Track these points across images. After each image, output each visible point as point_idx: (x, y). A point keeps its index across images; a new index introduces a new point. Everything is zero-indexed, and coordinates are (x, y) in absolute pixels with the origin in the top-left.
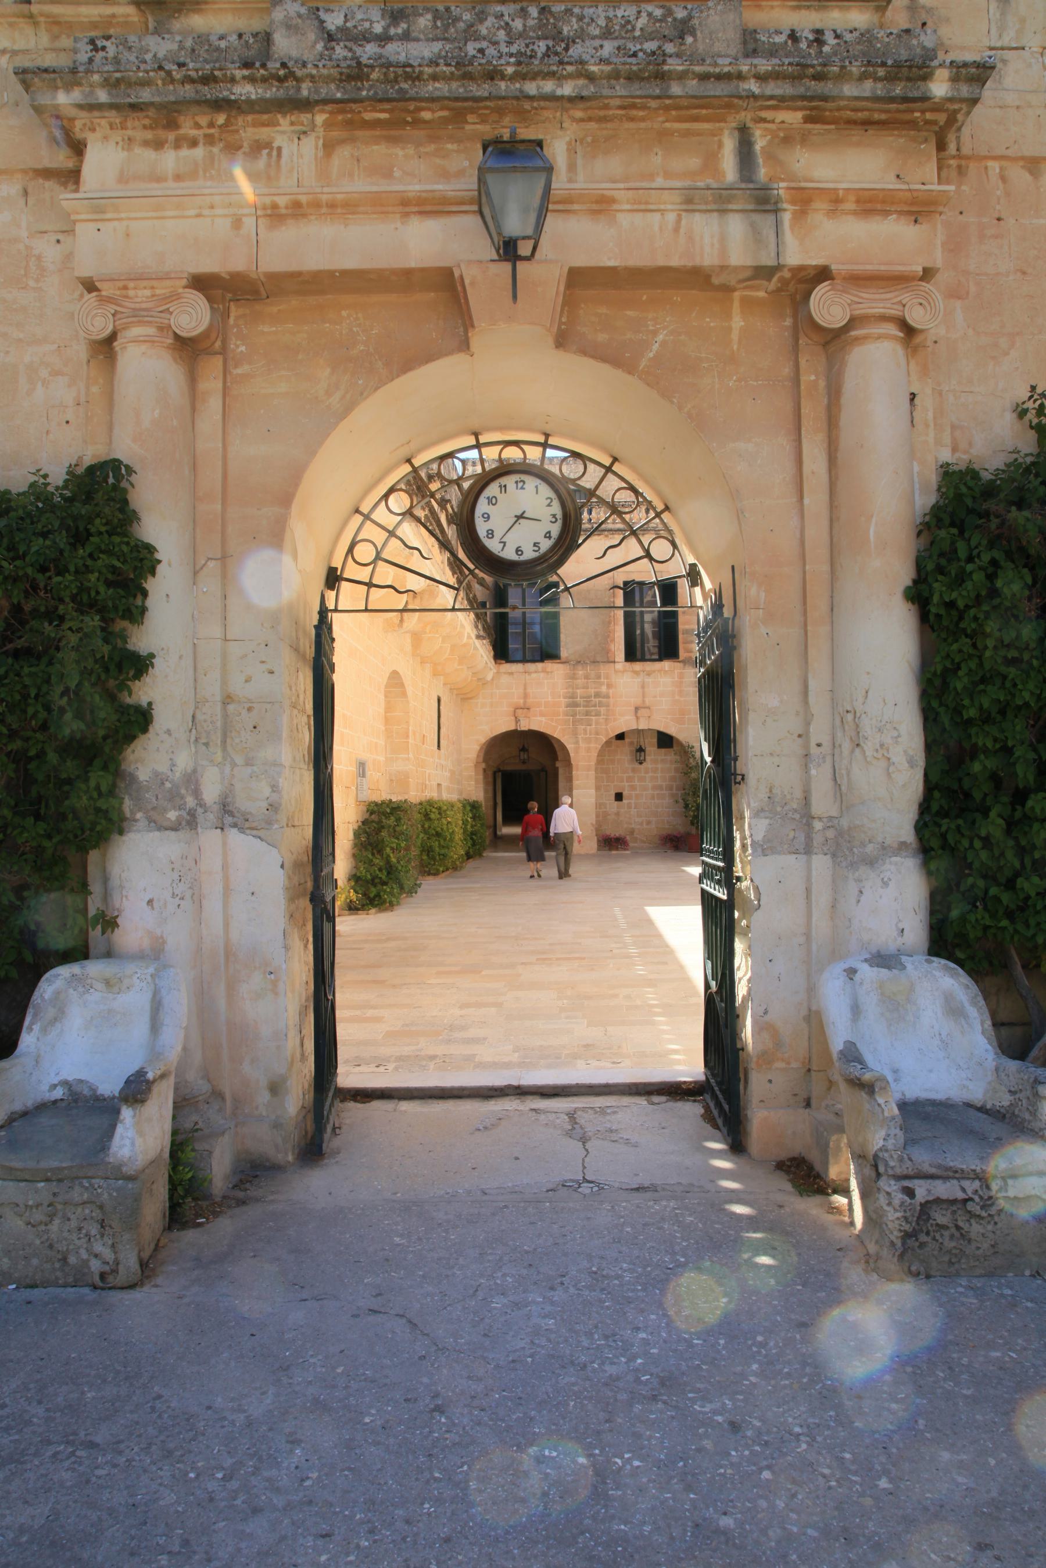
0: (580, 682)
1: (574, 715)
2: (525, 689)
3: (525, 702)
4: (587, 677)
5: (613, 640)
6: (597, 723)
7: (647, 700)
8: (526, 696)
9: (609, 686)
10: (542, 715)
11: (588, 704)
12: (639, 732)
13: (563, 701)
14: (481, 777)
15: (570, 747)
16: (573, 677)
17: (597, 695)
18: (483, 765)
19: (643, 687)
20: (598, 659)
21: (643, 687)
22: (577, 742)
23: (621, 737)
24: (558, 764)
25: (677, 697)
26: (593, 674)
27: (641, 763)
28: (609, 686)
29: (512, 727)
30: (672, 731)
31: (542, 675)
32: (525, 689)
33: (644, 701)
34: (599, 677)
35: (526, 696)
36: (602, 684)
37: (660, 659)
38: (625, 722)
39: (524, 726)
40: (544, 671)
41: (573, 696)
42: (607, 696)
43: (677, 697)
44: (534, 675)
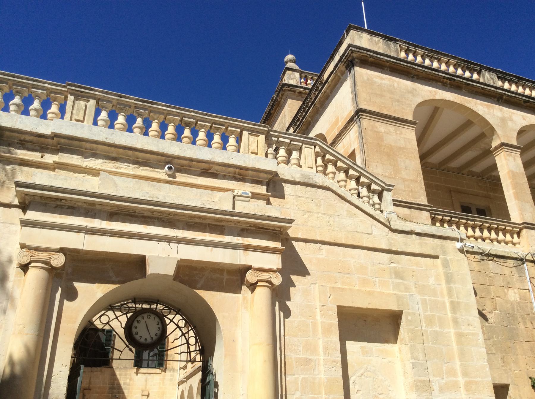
3: (89, 386)
7: (147, 387)
8: (90, 383)
10: (97, 393)
13: (108, 386)
19: (146, 381)
21: (146, 381)
25: (161, 386)
28: (131, 380)
31: (99, 373)
33: (146, 387)
34: (126, 375)
35: (90, 383)
36: (127, 378)
37: (155, 368)
40: (101, 371)
42: (129, 385)
44: (95, 373)
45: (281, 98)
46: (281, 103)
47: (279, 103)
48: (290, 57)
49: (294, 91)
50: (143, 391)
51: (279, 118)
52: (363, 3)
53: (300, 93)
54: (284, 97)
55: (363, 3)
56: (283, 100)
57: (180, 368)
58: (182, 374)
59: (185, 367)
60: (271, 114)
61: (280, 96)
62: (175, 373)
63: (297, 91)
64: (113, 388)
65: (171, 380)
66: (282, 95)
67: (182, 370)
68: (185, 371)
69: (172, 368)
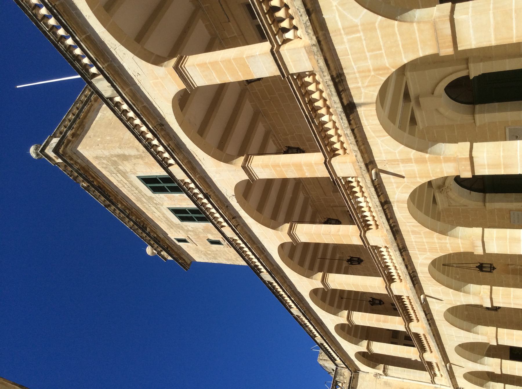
45: (76, 163)
46: (84, 165)
47: (83, 168)
48: (32, 150)
49: (69, 141)
51: (99, 167)
52: (18, 87)
53: (73, 135)
54: (74, 157)
55: (18, 87)
56: (79, 161)
60: (99, 187)
61: (72, 162)
63: (70, 138)
66: (71, 159)
67: (436, 379)
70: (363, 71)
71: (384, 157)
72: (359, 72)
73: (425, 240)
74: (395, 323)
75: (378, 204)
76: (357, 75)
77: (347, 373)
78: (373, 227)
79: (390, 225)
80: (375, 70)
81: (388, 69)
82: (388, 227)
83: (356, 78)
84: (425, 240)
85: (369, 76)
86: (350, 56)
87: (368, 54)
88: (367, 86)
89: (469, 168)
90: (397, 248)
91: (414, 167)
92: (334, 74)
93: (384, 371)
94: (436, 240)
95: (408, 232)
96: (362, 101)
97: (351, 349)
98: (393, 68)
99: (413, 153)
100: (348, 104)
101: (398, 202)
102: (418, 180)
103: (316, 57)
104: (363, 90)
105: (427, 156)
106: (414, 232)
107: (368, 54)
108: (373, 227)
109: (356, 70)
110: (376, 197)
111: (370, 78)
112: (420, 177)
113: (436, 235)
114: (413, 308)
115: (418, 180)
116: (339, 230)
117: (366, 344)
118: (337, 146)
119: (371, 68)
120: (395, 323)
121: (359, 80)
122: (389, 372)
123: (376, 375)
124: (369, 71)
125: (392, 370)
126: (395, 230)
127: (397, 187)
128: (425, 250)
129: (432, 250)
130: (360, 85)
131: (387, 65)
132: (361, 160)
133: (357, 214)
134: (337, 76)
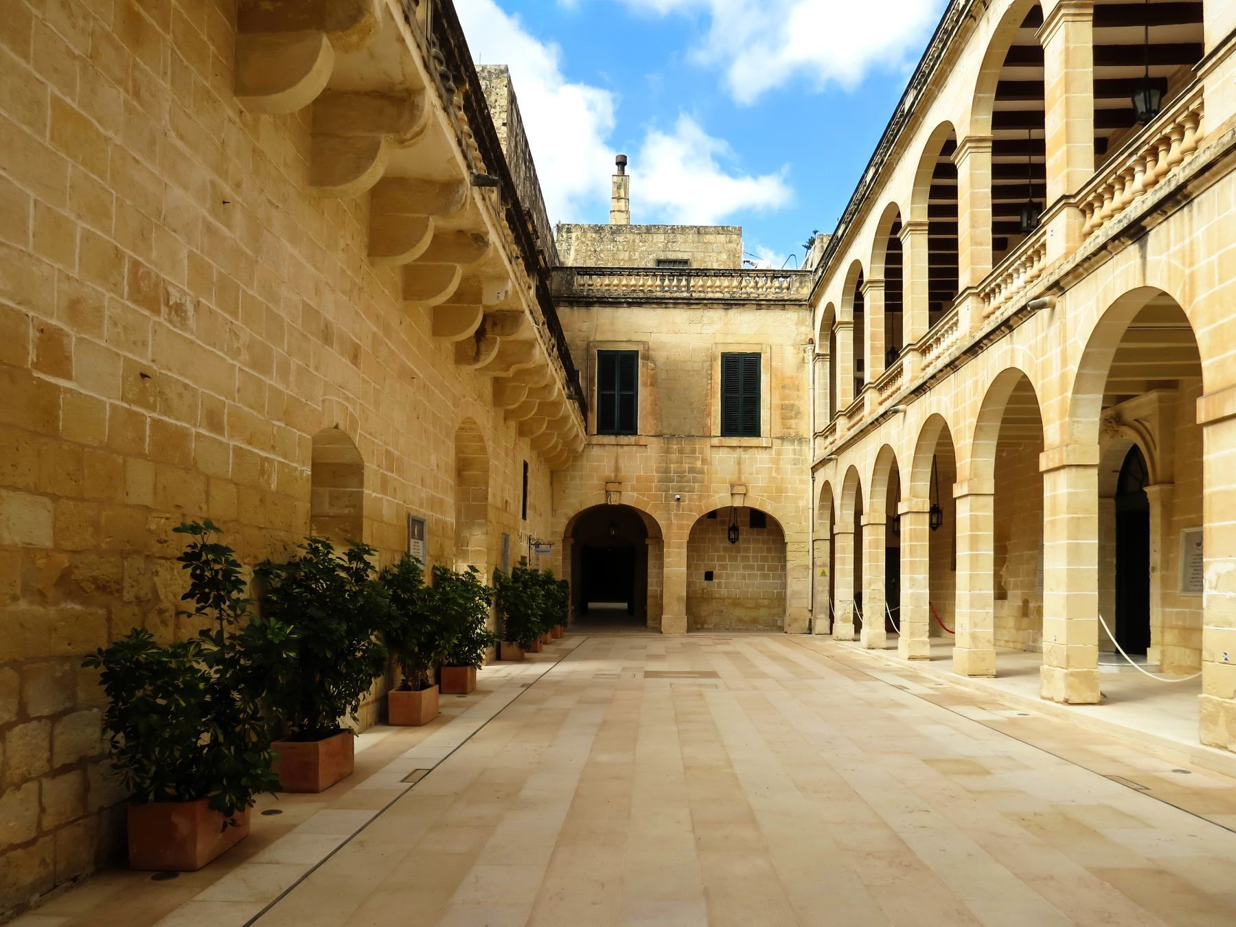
0: (674, 456)
1: (667, 490)
2: (617, 462)
3: (616, 476)
4: (681, 452)
5: (709, 415)
6: (690, 500)
8: (617, 469)
9: (704, 461)
10: (633, 489)
11: (681, 478)
12: (734, 510)
14: (569, 552)
15: (662, 523)
16: (668, 451)
17: (692, 470)
18: (572, 541)
20: (693, 433)
21: (739, 463)
22: (669, 519)
23: (713, 515)
24: (648, 541)
25: (774, 474)
26: (688, 448)
27: (733, 542)
29: (603, 502)
30: (768, 508)
31: (634, 448)
32: (617, 462)
33: (739, 478)
34: (694, 452)
38: (721, 499)
39: (615, 500)
41: (667, 471)
42: (703, 473)
43: (774, 474)
50: (732, 486)
57: (816, 435)
58: (822, 448)
59: (832, 429)
62: (805, 447)
64: (670, 480)
65: (796, 462)
68: (830, 439)
69: (797, 434)
70: (1192, 251)
71: (1070, 315)
72: (1192, 243)
73: (967, 403)
74: (874, 367)
75: (1006, 316)
76: (1187, 241)
77: (806, 292)
78: (988, 308)
79: (980, 341)
80: (1192, 274)
81: (1191, 301)
82: (977, 339)
83: (1182, 238)
84: (967, 403)
85: (1184, 264)
86: (1217, 218)
87: (1215, 257)
88: (1169, 265)
89: (1051, 466)
90: (953, 358)
91: (1055, 375)
92: (1190, 188)
93: (818, 355)
94: (967, 423)
95: (976, 374)
96: (1149, 258)
97: (835, 292)
98: (1192, 312)
99: (1074, 368)
100: (1144, 228)
101: (1013, 350)
102: (1040, 383)
103: (1214, 143)
104: (1165, 256)
105: (1069, 394)
106: (976, 383)
107: (1215, 257)
108: (988, 308)
109: (1195, 235)
110: (1014, 310)
111: (1181, 267)
112: (1043, 385)
113: (975, 421)
114: (894, 393)
115: (1040, 383)
116: (981, 244)
117: (846, 320)
118: (1098, 214)
119: (1195, 267)
120: (874, 367)
121: (1178, 247)
122: (818, 365)
123: (811, 342)
124: (1191, 264)
125: (823, 368)
126: (974, 349)
127: (1030, 348)
128: (956, 406)
129: (956, 415)
130: (1173, 249)
131: (1196, 300)
132: (1063, 273)
133: (1000, 275)
134: (1186, 197)
